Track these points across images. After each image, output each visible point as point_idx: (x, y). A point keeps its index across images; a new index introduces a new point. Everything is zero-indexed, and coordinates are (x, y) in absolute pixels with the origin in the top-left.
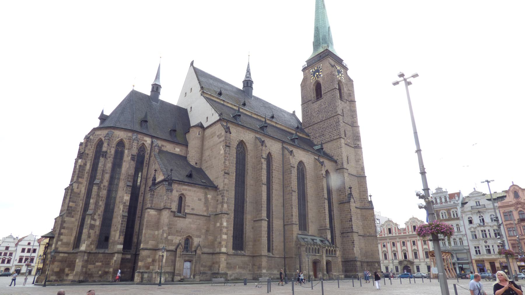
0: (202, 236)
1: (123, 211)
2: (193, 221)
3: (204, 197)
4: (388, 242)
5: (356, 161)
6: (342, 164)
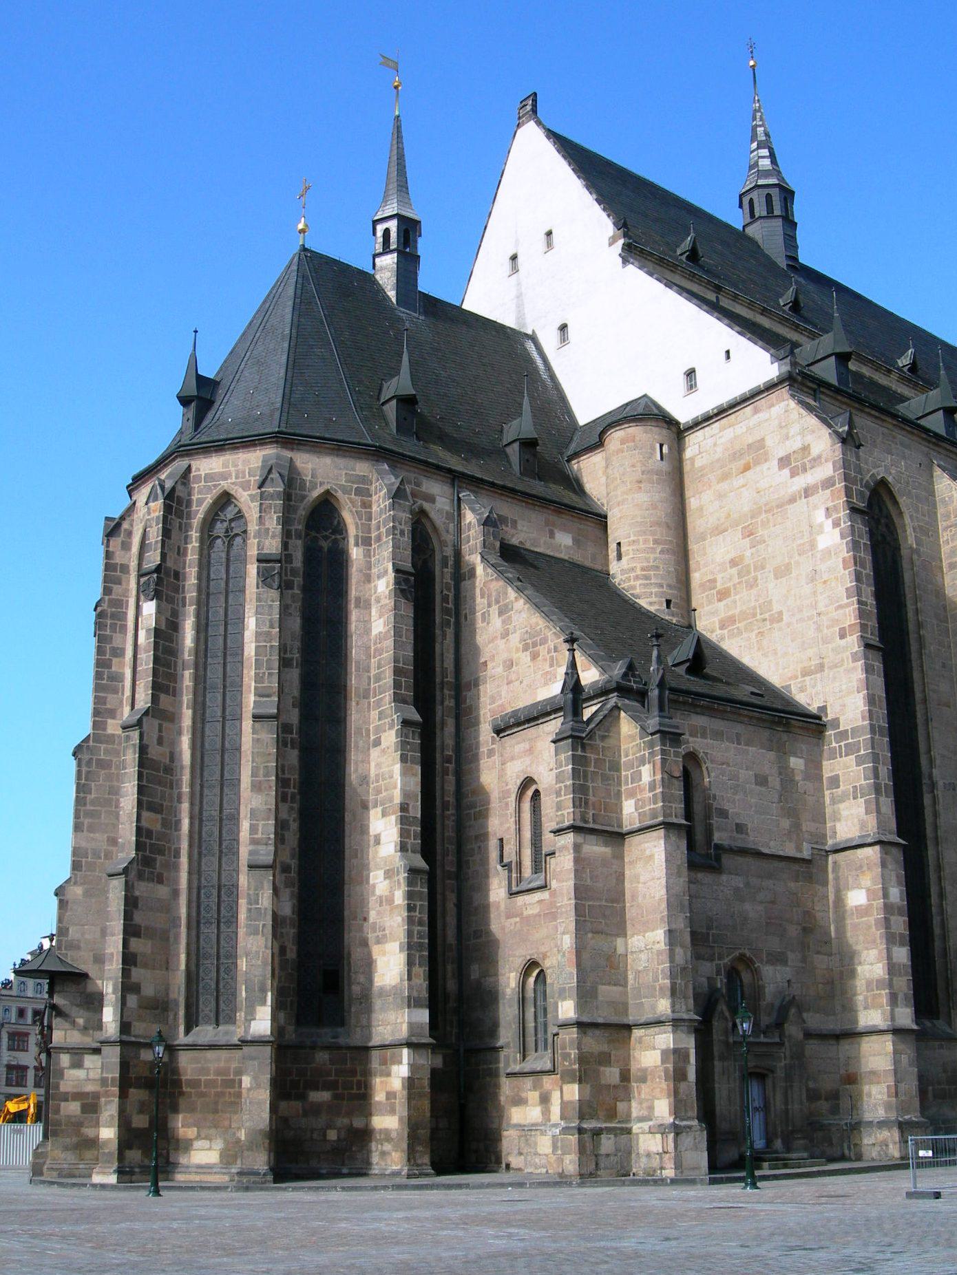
0: (791, 956)
1: (403, 848)
2: (747, 884)
3: (775, 770)
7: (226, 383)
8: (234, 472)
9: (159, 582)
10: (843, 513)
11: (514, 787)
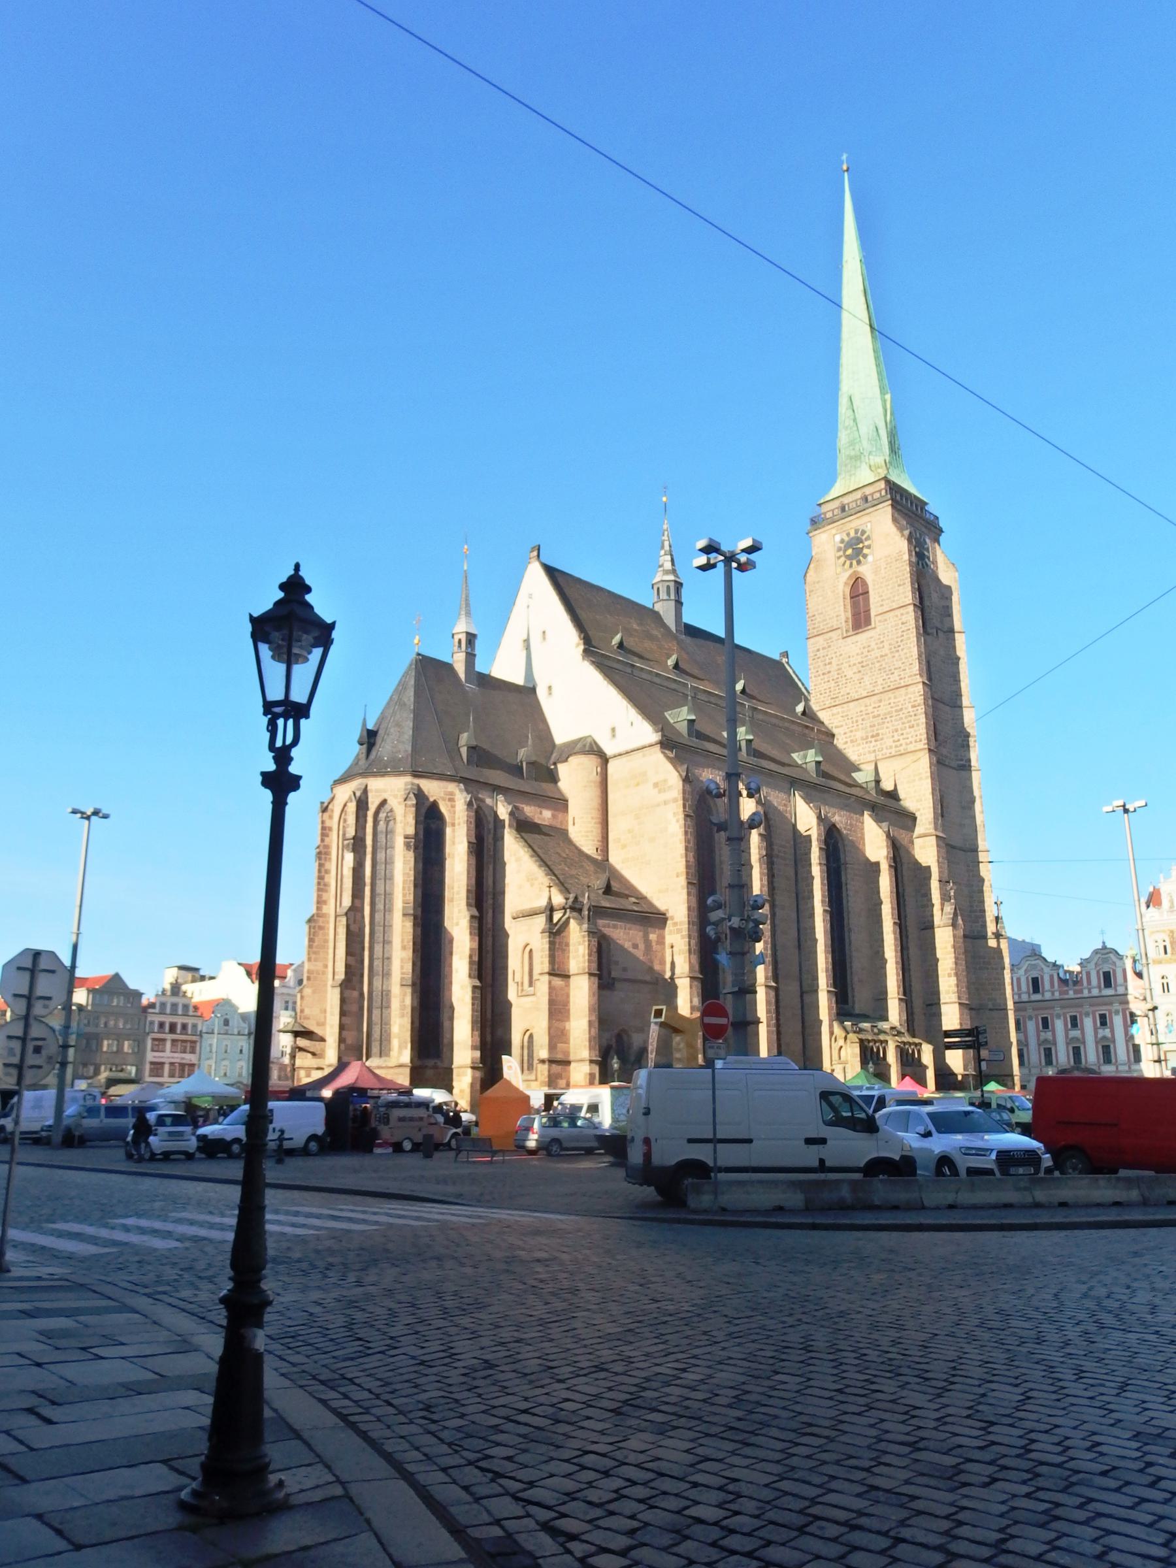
4: (1030, 1018)
7: (381, 733)
8: (391, 790)
9: (354, 845)
10: (681, 816)
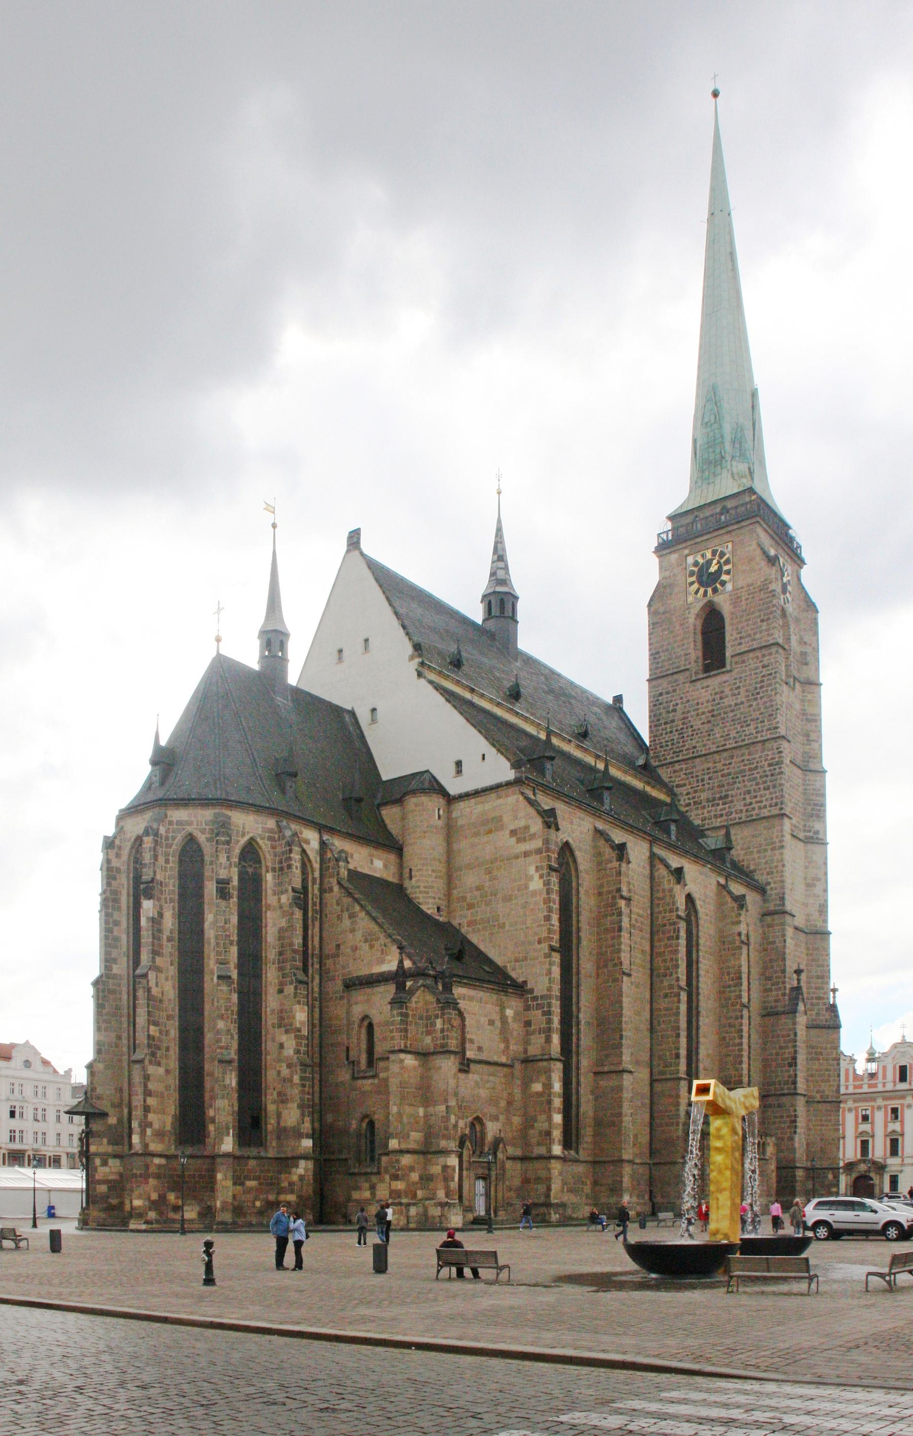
1: (297, 1052)
5: (808, 885)
6: (782, 899)
11: (357, 1022)
